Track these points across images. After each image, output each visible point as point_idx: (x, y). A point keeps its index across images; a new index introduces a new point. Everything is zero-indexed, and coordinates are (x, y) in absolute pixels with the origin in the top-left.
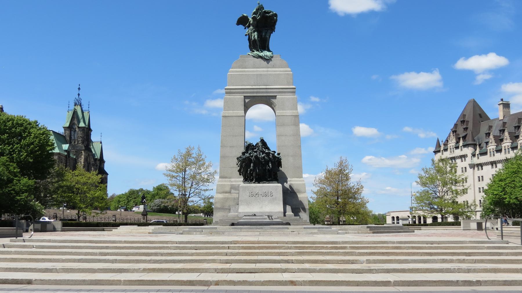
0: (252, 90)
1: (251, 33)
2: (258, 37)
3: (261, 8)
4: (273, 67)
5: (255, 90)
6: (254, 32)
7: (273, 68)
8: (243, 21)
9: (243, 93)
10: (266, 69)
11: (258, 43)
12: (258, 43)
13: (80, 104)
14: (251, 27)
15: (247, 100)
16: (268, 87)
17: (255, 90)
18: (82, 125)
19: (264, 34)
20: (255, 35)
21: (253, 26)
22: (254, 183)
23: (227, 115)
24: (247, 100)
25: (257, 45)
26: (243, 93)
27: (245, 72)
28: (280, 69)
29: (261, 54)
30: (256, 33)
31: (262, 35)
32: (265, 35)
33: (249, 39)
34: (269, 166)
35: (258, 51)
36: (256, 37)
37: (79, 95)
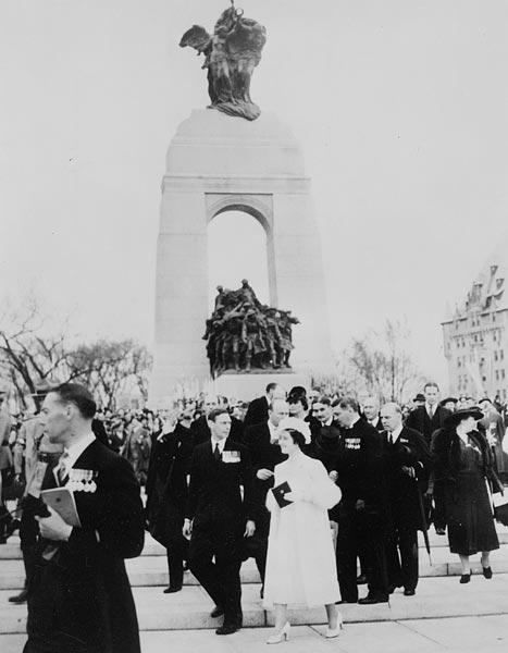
3: (229, 15)
8: (193, 36)
14: (214, 52)
30: (225, 64)
31: (236, 70)
34: (277, 338)
35: (230, 100)
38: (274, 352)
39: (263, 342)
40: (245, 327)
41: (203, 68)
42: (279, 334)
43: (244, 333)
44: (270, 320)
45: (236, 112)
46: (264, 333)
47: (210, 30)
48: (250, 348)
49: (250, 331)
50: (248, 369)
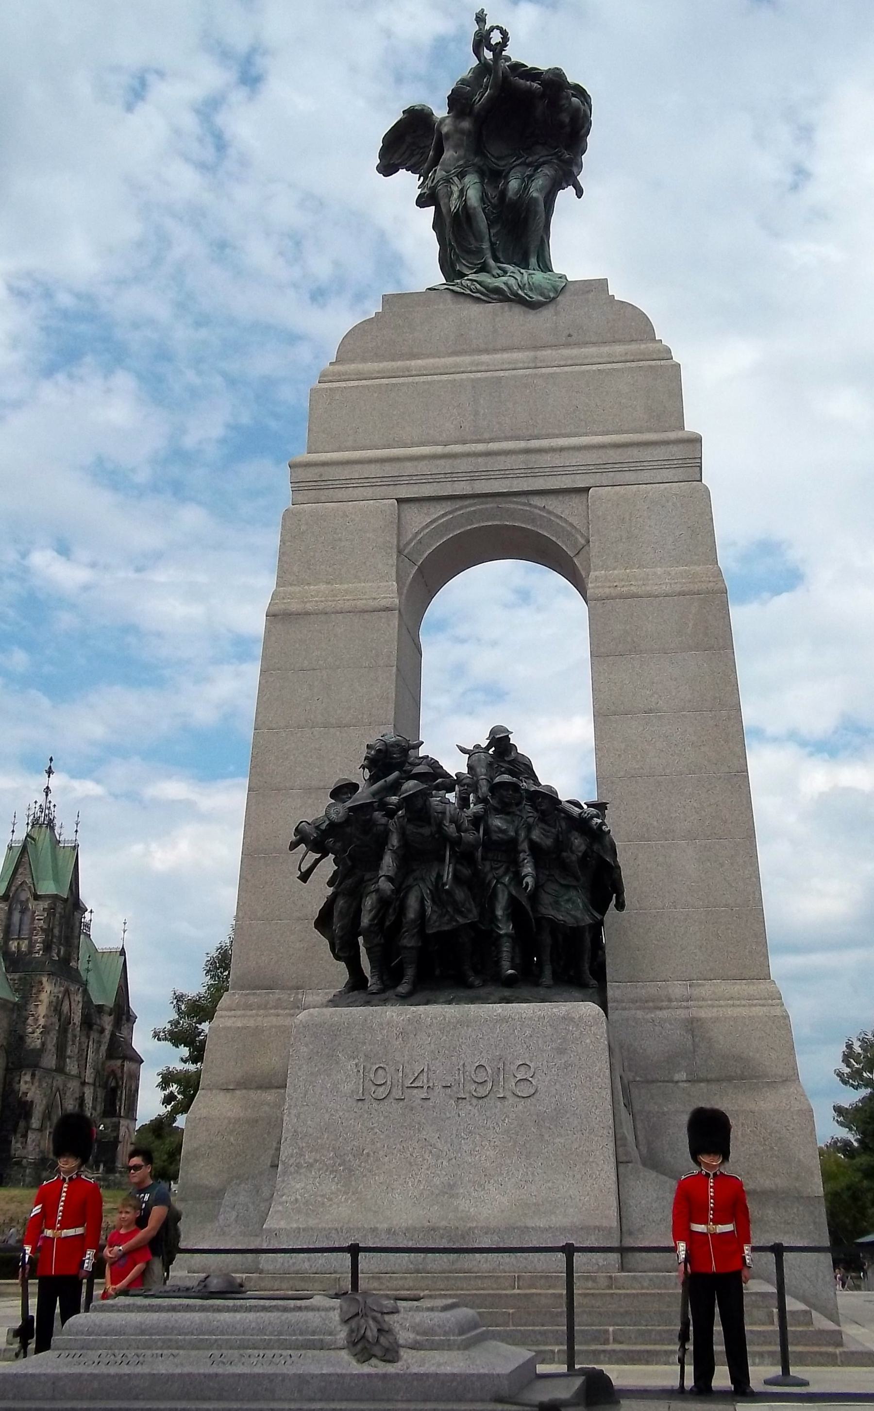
0: (445, 466)
1: (448, 181)
2: (484, 198)
4: (570, 339)
5: (464, 465)
6: (461, 175)
7: (567, 345)
8: (408, 143)
9: (395, 481)
10: (531, 354)
11: (482, 222)
12: (482, 222)
13: (51, 821)
15: (418, 519)
16: (534, 444)
17: (464, 465)
18: (48, 887)
19: (514, 184)
20: (472, 190)
21: (456, 148)
22: (405, 999)
23: (295, 607)
24: (418, 519)
25: (479, 238)
26: (395, 481)
27: (407, 373)
28: (605, 349)
29: (499, 282)
30: (471, 179)
31: (503, 194)
32: (525, 188)
33: (438, 225)
34: (518, 878)
35: (483, 268)
36: (473, 195)
37: (47, 790)
38: (506, 928)
39: (460, 895)
40: (394, 841)
41: (422, 202)
42: (528, 869)
43: (388, 862)
44: (497, 822)
45: (497, 291)
46: (465, 856)
47: (440, 112)
48: (411, 915)
49: (409, 858)
50: (402, 989)
